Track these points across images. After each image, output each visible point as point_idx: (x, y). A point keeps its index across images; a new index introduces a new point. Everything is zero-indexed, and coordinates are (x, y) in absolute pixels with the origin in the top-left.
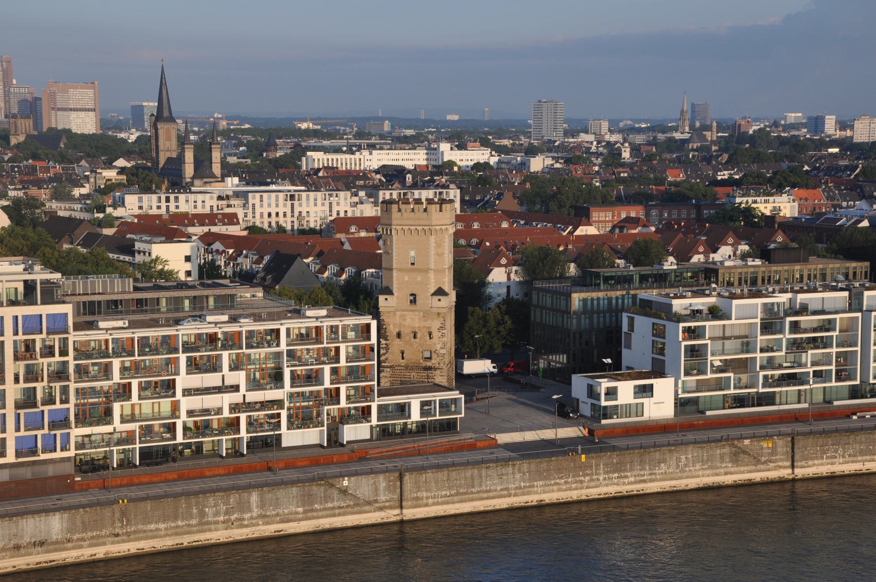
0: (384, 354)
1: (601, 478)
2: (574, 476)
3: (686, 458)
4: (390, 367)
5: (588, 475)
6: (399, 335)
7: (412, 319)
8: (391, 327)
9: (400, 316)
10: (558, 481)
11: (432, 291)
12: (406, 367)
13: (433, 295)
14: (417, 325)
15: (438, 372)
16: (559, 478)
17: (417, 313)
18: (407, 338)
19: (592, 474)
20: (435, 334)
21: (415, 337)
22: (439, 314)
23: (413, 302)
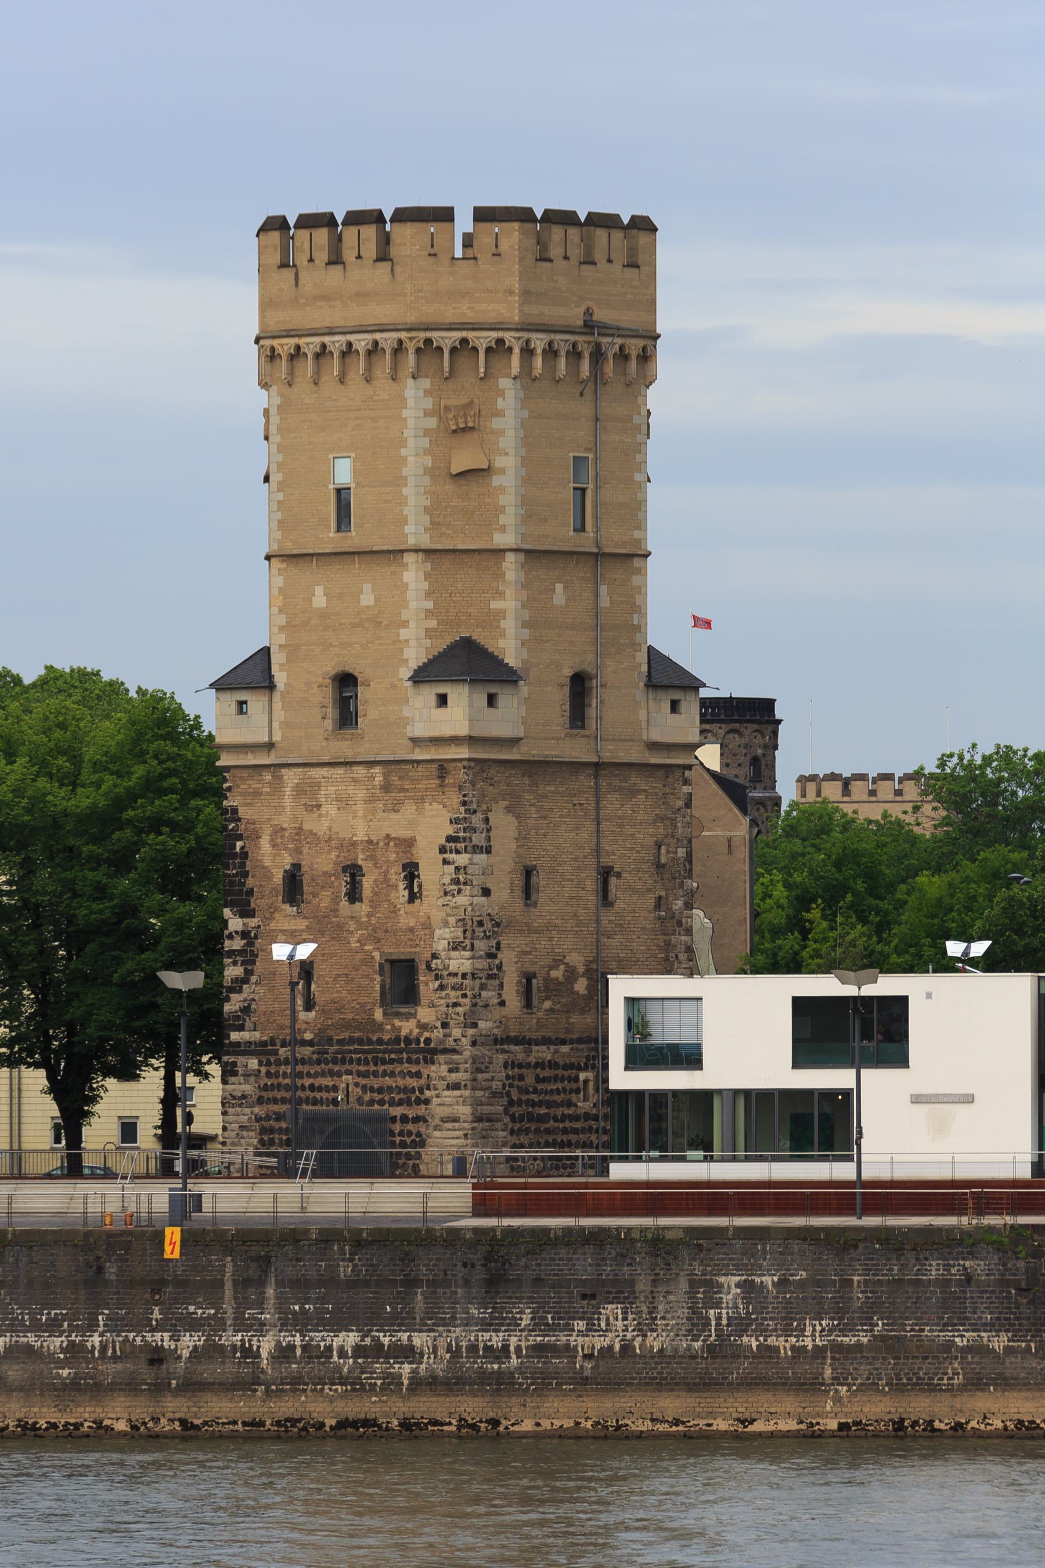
0: (238, 984)
1: (266, 1346)
2: (115, 1325)
3: (748, 1287)
4: (261, 1049)
5: (193, 1325)
6: (293, 886)
7: (344, 802)
8: (265, 843)
9: (299, 791)
10: (31, 1338)
11: (415, 656)
12: (322, 1041)
13: (421, 677)
14: (361, 836)
15: (439, 1070)
16: (36, 1327)
17: (360, 771)
18: (324, 901)
19: (218, 1324)
20: (433, 874)
21: (354, 895)
22: (442, 768)
23: (347, 715)
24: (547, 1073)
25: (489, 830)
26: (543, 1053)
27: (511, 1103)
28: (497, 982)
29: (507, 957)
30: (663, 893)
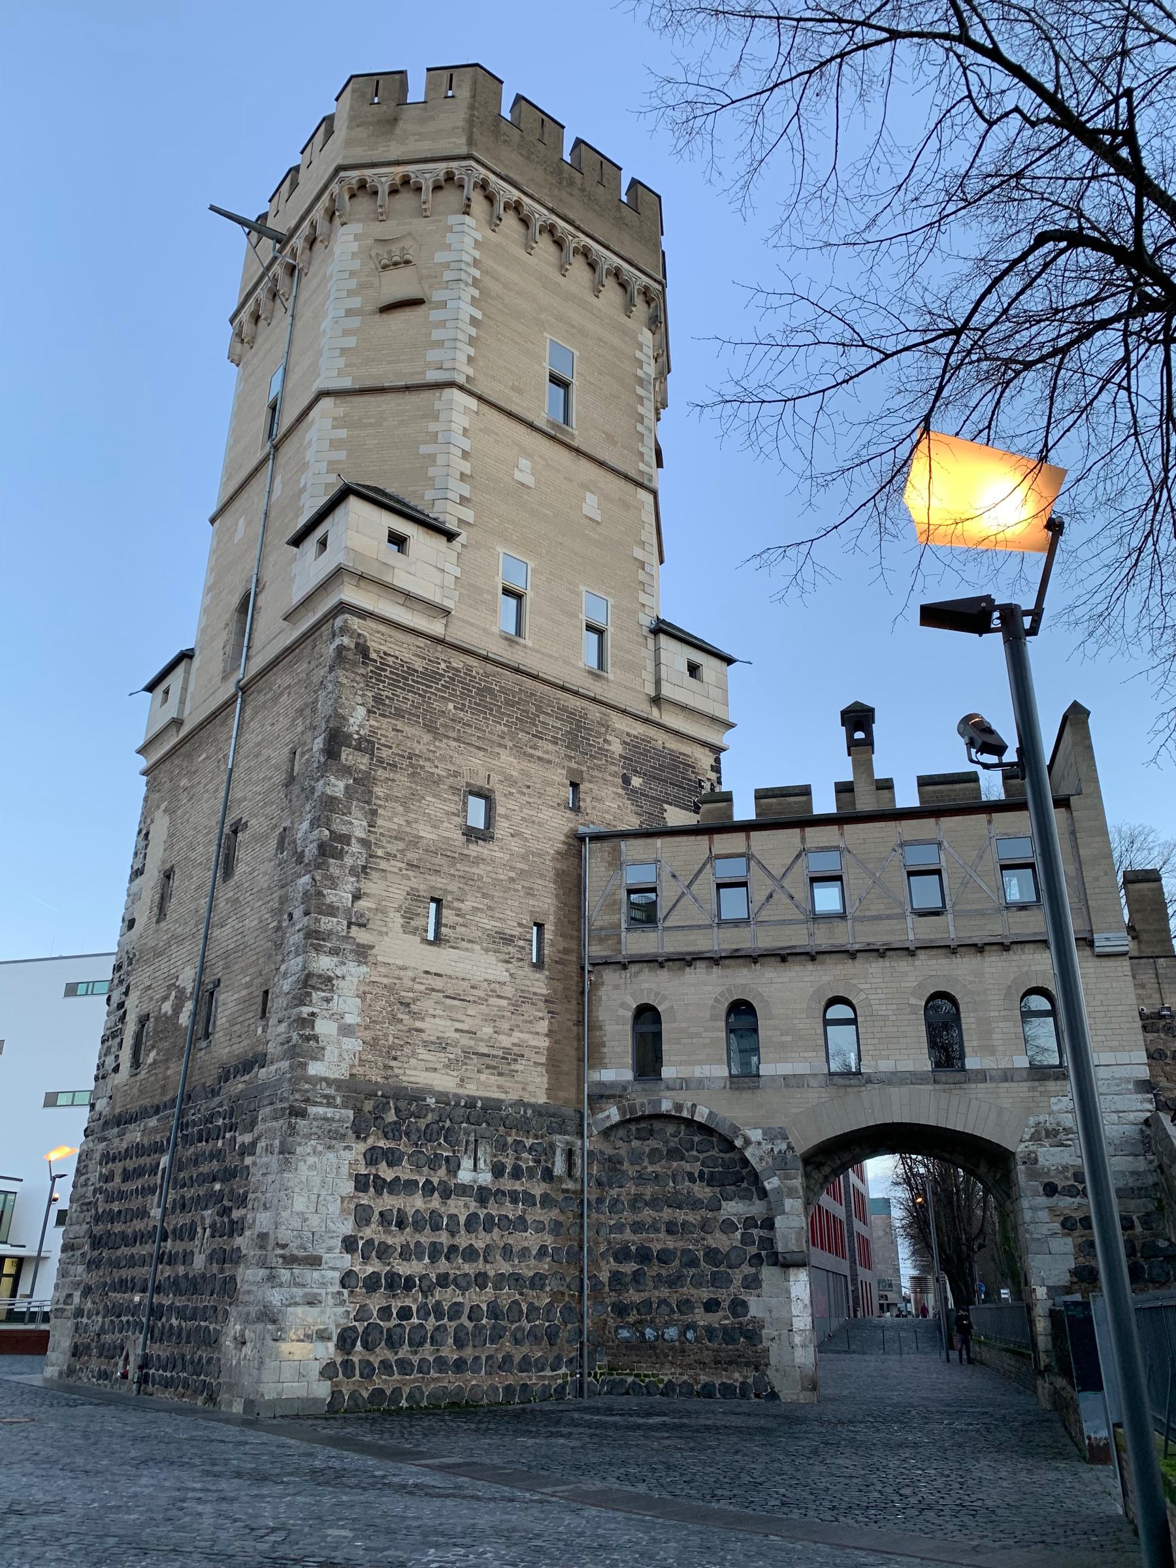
24: (131, 1164)
25: (147, 846)
26: (135, 1135)
27: (97, 1219)
28: (118, 1040)
29: (131, 1003)
30: (287, 824)
